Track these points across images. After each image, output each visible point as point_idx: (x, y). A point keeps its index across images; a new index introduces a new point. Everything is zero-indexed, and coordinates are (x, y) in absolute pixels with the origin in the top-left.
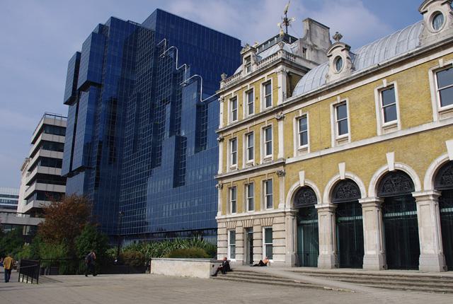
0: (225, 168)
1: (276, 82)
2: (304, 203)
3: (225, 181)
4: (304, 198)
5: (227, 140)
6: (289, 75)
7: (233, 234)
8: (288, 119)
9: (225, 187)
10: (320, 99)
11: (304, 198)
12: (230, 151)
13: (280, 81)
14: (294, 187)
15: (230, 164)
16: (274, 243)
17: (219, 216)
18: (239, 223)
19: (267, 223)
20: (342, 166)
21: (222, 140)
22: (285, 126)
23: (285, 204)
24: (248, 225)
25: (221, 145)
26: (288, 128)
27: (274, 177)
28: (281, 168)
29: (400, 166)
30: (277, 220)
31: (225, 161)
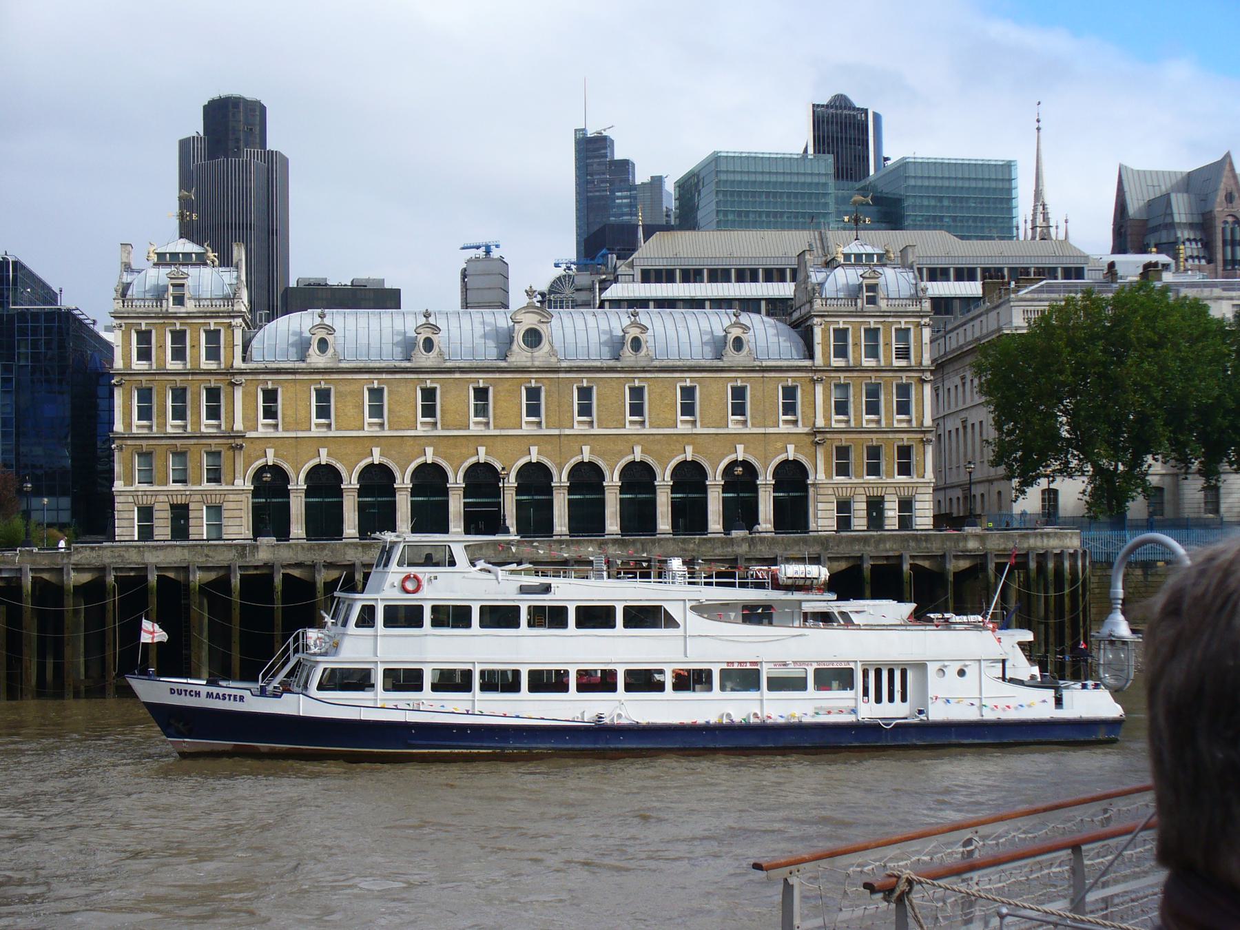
0: (128, 425)
2: (271, 485)
3: (129, 442)
10: (298, 377)
16: (224, 522)
17: (118, 485)
18: (161, 498)
21: (120, 385)
23: (244, 484)
25: (118, 394)
26: (249, 398)
28: (239, 441)
29: (385, 461)
30: (231, 497)
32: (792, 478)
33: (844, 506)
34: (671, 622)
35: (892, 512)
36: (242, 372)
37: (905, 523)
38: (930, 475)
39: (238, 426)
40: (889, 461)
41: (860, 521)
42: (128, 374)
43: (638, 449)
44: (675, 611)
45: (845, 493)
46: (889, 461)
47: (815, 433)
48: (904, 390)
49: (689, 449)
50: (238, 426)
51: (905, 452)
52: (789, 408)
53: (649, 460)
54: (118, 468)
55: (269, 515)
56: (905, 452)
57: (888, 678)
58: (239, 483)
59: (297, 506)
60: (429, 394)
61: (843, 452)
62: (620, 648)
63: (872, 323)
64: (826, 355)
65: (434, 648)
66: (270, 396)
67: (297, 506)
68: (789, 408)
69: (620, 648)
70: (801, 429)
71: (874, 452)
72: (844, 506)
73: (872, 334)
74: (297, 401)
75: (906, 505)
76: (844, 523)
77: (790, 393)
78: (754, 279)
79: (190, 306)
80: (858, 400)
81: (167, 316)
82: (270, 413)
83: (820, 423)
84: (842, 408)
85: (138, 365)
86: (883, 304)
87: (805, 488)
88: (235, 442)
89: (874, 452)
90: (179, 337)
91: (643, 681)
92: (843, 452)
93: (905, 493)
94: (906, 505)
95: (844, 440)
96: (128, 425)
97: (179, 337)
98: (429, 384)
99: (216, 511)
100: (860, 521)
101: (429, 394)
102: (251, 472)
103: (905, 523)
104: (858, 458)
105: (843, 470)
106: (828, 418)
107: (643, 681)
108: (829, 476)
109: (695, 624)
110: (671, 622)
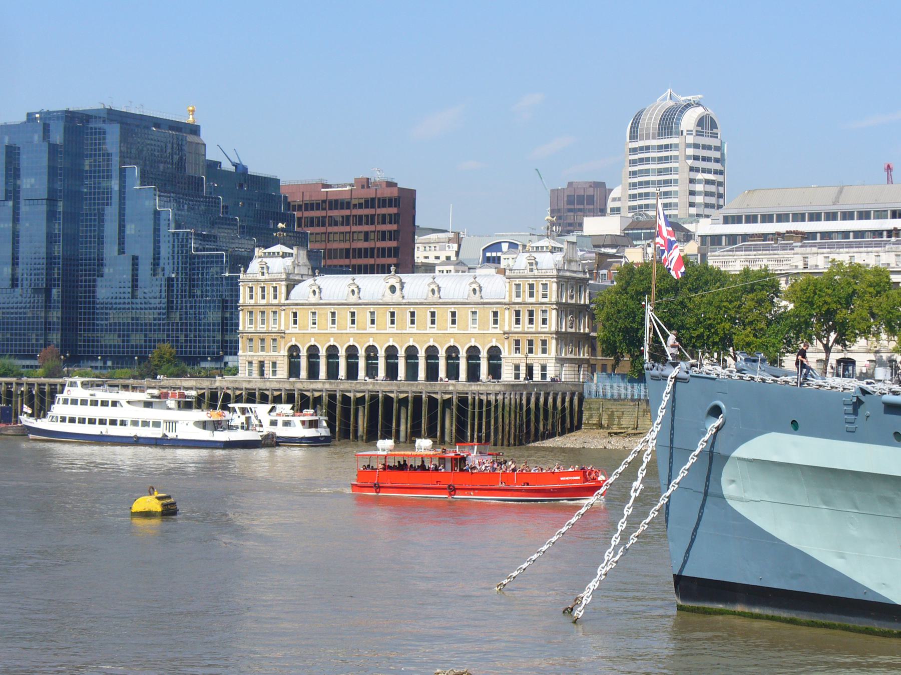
0: (244, 327)
1: (281, 289)
4: (294, 349)
5: (246, 311)
6: (287, 286)
7: (250, 363)
8: (287, 311)
9: (245, 338)
11: (294, 349)
12: (247, 317)
13: (283, 289)
14: (290, 344)
15: (247, 325)
17: (240, 353)
19: (274, 360)
20: (313, 339)
22: (286, 314)
23: (284, 352)
24: (261, 359)
25: (241, 313)
26: (287, 315)
27: (278, 338)
31: (244, 323)
32: (494, 354)
33: (517, 368)
37: (544, 376)
40: (537, 347)
41: (523, 375)
43: (432, 340)
45: (517, 362)
46: (537, 347)
47: (504, 334)
50: (282, 328)
51: (544, 342)
52: (496, 322)
54: (240, 345)
56: (544, 342)
57: (172, 424)
61: (517, 342)
62: (108, 413)
63: (531, 281)
64: (510, 296)
68: (496, 322)
69: (108, 413)
70: (498, 331)
72: (517, 368)
73: (531, 286)
74: (305, 316)
75: (544, 368)
76: (517, 376)
77: (495, 314)
78: (771, 221)
79: (266, 276)
80: (525, 317)
82: (295, 322)
83: (507, 329)
84: (518, 322)
85: (249, 302)
88: (282, 333)
89: (531, 343)
90: (263, 289)
91: (113, 422)
92: (517, 342)
93: (542, 362)
94: (544, 368)
95: (516, 337)
96: (244, 327)
98: (352, 310)
99: (274, 364)
100: (537, 377)
102: (287, 348)
103: (544, 376)
104: (524, 346)
106: (510, 327)
107: (113, 422)
108: (510, 353)
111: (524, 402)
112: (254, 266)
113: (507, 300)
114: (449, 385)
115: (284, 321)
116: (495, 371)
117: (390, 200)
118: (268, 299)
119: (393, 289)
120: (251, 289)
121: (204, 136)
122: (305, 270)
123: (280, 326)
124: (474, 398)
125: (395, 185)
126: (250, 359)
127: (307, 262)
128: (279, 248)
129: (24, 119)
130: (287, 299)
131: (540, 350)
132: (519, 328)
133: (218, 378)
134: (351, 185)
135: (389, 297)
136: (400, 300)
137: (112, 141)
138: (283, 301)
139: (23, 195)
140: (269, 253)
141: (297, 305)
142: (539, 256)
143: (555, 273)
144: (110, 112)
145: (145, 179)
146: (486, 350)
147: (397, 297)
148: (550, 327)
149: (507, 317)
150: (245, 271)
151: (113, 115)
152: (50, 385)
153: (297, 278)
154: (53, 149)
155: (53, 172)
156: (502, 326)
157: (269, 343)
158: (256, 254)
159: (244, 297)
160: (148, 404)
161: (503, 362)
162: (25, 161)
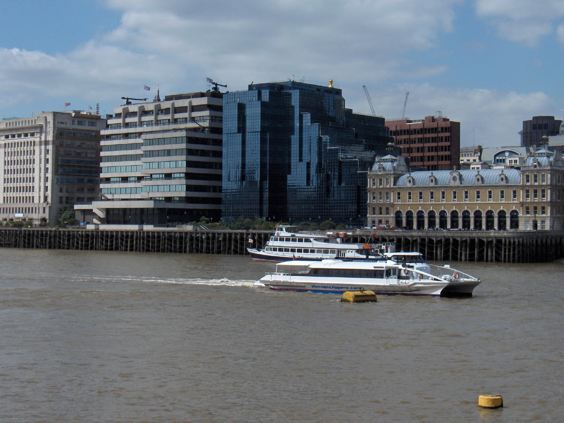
0: (370, 201)
4: (398, 214)
6: (394, 178)
11: (398, 214)
13: (392, 180)
14: (396, 210)
17: (368, 215)
24: (380, 219)
27: (390, 207)
34: (311, 242)
35: (539, 224)
36: (393, 188)
37: (543, 227)
38: (549, 214)
39: (392, 201)
40: (539, 210)
42: (371, 190)
44: (312, 239)
46: (539, 210)
48: (543, 191)
49: (490, 207)
53: (481, 210)
55: (398, 223)
56: (543, 208)
58: (392, 215)
59: (437, 221)
60: (432, 193)
61: (527, 208)
65: (278, 244)
66: (399, 194)
67: (437, 221)
68: (515, 196)
70: (516, 202)
71: (535, 208)
73: (535, 176)
80: (531, 193)
81: (378, 175)
82: (399, 198)
83: (521, 200)
86: (538, 168)
87: (518, 217)
88: (393, 205)
89: (535, 208)
90: (381, 180)
92: (527, 208)
93: (543, 219)
94: (543, 222)
97: (381, 180)
101: (432, 193)
102: (394, 212)
103: (543, 227)
104: (531, 210)
105: (528, 213)
109: (315, 242)
110: (311, 242)
111: (535, 242)
112: (376, 167)
113: (521, 184)
114: (490, 233)
115: (392, 198)
116: (515, 224)
117: (446, 128)
118: (384, 185)
119: (454, 179)
120: (374, 180)
121: (344, 95)
122: (403, 168)
123: (390, 200)
124: (506, 241)
125: (448, 120)
126: (373, 219)
127: (405, 164)
128: (388, 157)
129: (247, 89)
130: (395, 184)
131: (541, 212)
132: (529, 200)
133: (358, 230)
134: (423, 120)
135: (452, 184)
136: (459, 184)
137: (295, 99)
138: (392, 186)
139: (247, 130)
140: (384, 159)
141: (400, 188)
142: (540, 159)
143: (549, 168)
144: (294, 83)
145: (313, 120)
146: (509, 213)
147: (457, 183)
148: (547, 199)
149: (521, 193)
150: (371, 170)
151: (295, 85)
152: (265, 234)
153: (401, 173)
154: (263, 105)
155: (264, 116)
156: (518, 199)
157: (384, 210)
158: (376, 160)
159: (370, 184)
160: (326, 241)
161: (520, 219)
162: (248, 112)
